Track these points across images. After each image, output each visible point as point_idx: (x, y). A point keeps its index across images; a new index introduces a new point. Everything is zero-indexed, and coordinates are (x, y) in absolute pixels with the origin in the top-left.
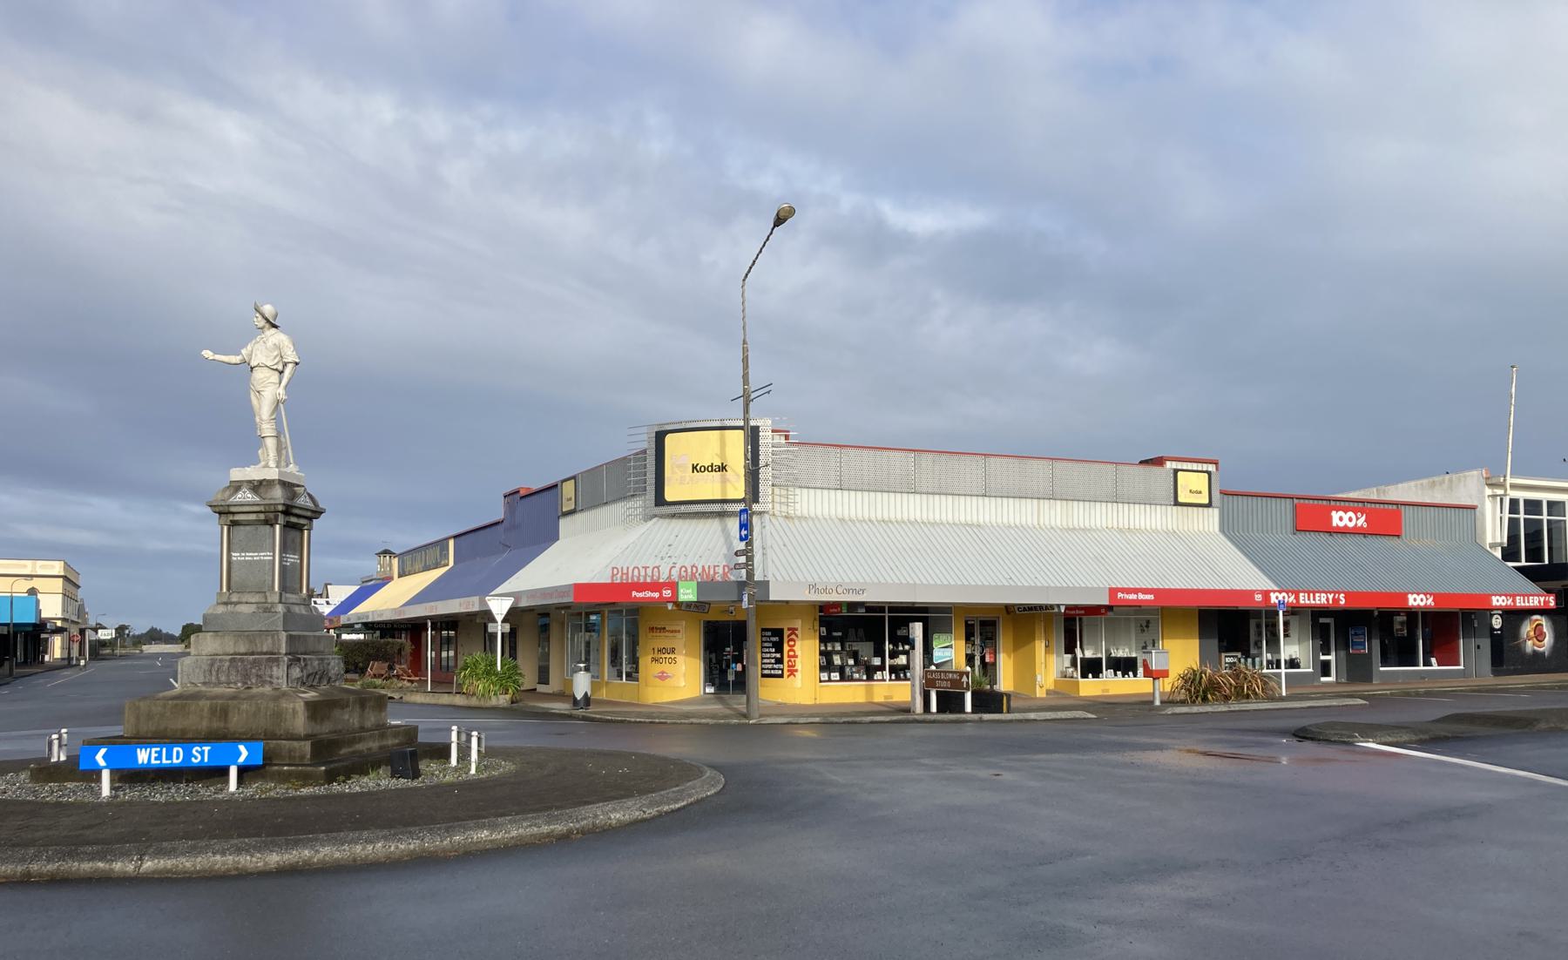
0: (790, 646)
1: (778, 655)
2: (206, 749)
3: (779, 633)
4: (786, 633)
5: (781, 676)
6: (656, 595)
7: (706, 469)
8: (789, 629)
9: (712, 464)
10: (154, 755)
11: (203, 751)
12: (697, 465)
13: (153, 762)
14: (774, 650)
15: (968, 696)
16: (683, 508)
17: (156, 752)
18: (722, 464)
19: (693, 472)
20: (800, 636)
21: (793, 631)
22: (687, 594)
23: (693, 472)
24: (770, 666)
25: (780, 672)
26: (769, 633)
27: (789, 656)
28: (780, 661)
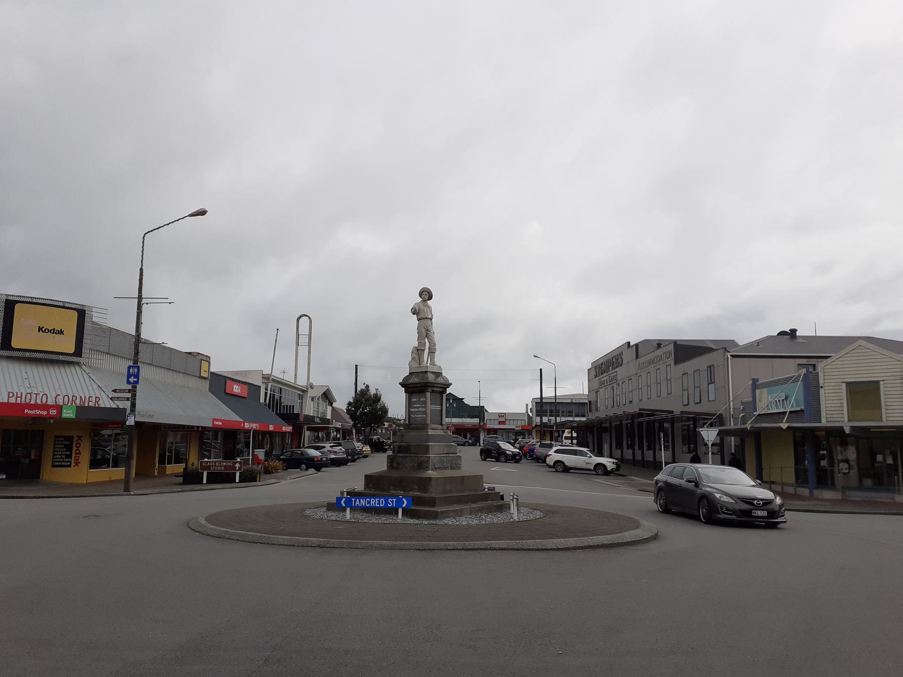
0: (76, 447)
1: (68, 453)
2: (394, 500)
3: (70, 439)
4: (75, 439)
5: (70, 466)
6: (45, 413)
7: (49, 331)
8: (77, 437)
9: (54, 329)
10: (377, 502)
11: (393, 501)
12: (43, 327)
13: (376, 505)
14: (65, 449)
15: (238, 474)
16: (27, 354)
17: (378, 501)
18: (61, 330)
19: (39, 331)
20: (83, 440)
21: (80, 437)
22: (68, 413)
23: (39, 331)
24: (61, 460)
25: (69, 464)
26: (62, 439)
27: (76, 453)
28: (70, 456)
